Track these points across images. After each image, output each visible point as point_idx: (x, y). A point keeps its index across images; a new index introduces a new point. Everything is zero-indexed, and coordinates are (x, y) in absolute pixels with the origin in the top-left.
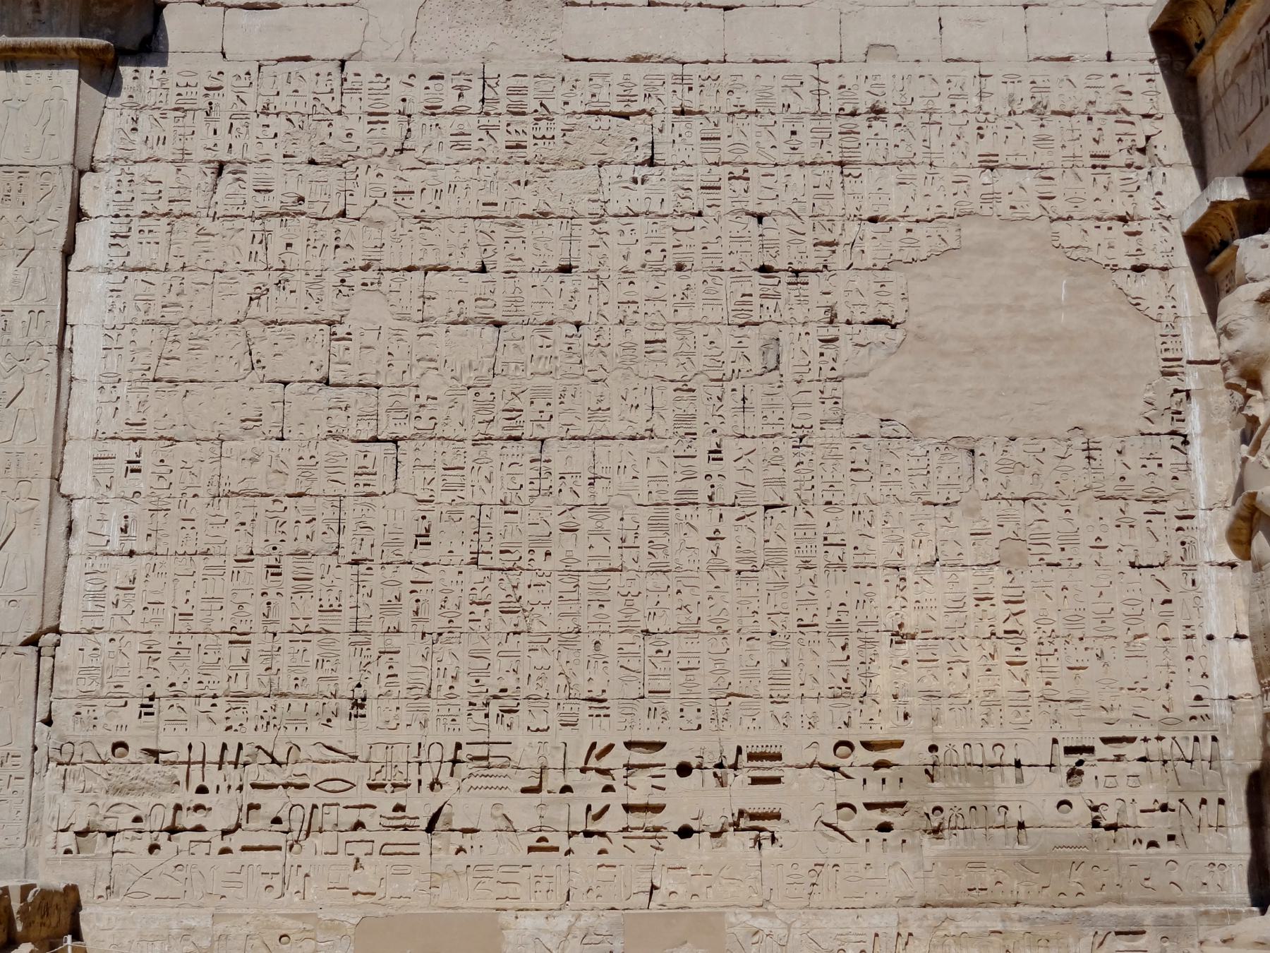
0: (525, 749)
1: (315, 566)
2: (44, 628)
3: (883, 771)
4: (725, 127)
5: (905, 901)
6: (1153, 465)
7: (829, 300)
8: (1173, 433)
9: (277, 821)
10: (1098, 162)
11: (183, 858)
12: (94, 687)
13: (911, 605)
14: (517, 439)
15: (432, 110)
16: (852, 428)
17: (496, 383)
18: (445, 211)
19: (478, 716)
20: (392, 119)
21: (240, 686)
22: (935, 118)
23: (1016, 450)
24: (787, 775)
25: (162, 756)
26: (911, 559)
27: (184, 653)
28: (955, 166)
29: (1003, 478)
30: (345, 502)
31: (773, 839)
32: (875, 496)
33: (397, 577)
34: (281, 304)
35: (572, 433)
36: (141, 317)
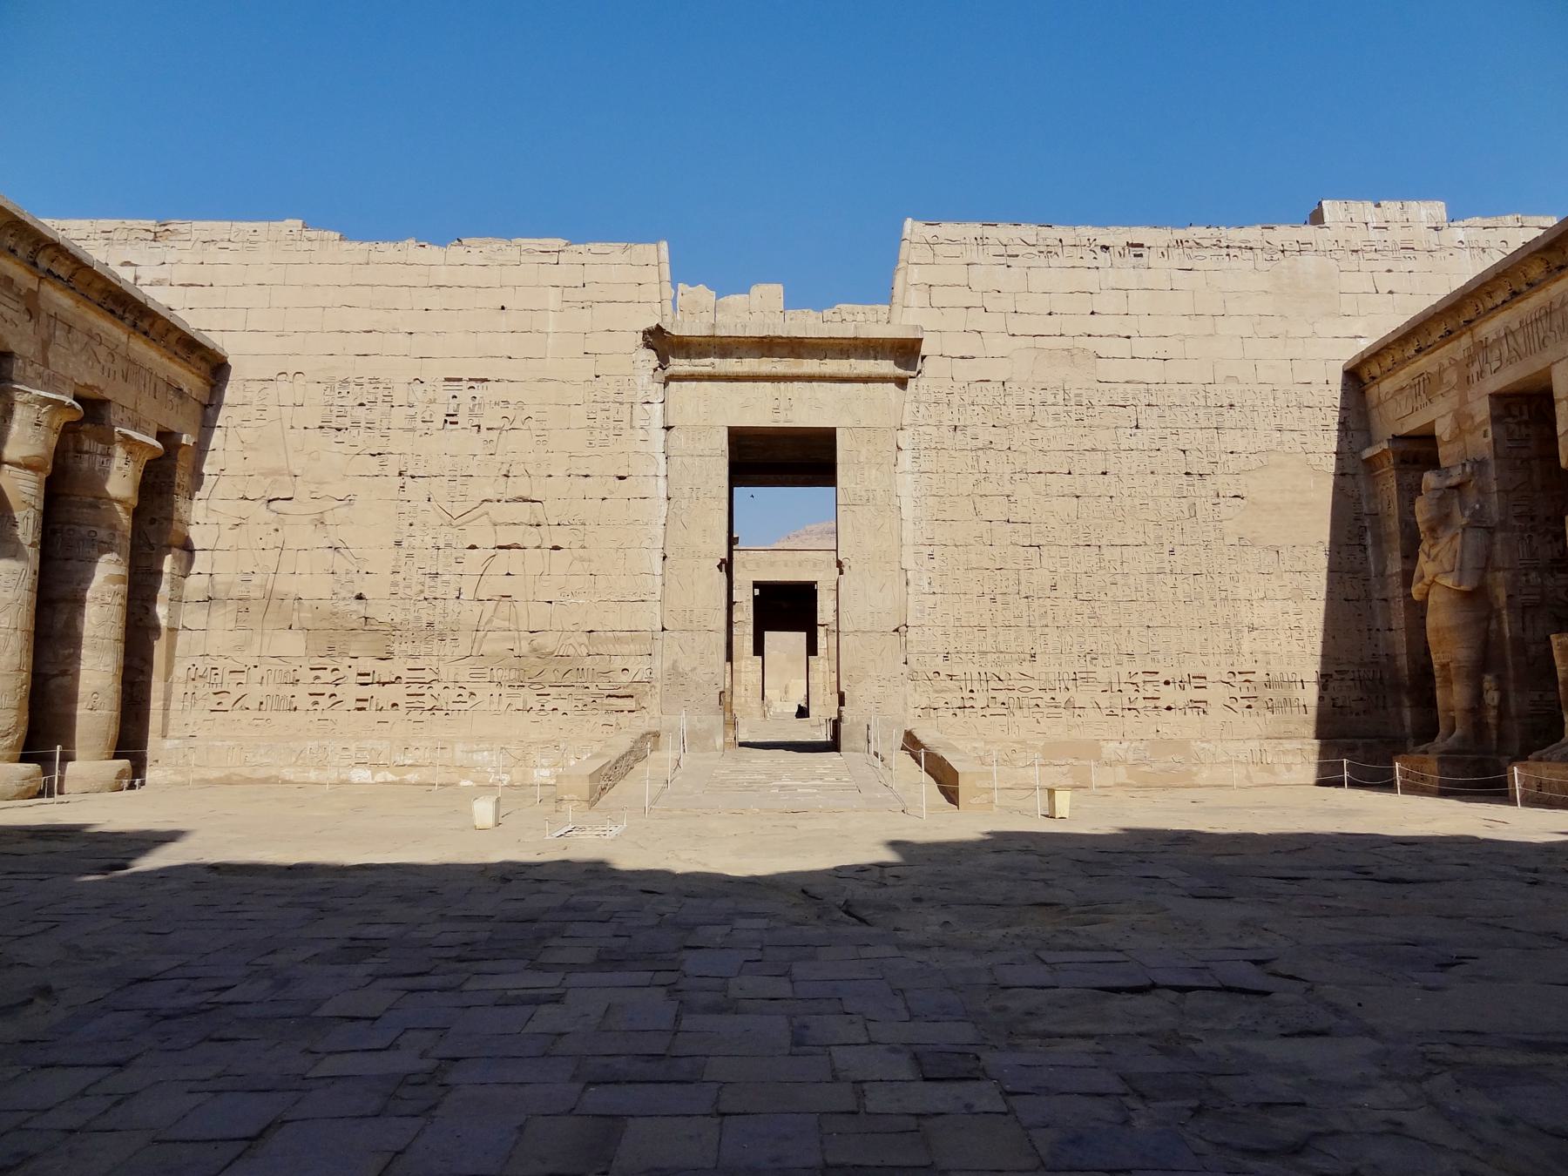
0: (1101, 674)
1: (1010, 598)
2: (901, 624)
3: (1248, 683)
4: (1167, 413)
5: (1259, 737)
6: (1352, 558)
7: (1214, 487)
8: (1359, 545)
9: (1003, 704)
10: (1325, 428)
11: (967, 719)
12: (923, 649)
13: (1256, 616)
14: (1089, 545)
15: (1043, 404)
16: (1228, 541)
17: (1080, 522)
18: (1051, 448)
19: (1082, 661)
20: (1027, 407)
21: (984, 649)
22: (1256, 408)
23: (1296, 551)
24: (1209, 685)
25: (954, 678)
26: (1255, 596)
27: (959, 635)
28: (1265, 430)
29: (1291, 563)
30: (1021, 572)
31: (1204, 712)
32: (1238, 570)
33: (1044, 603)
34: (987, 488)
35: (1113, 543)
36: (929, 493)
